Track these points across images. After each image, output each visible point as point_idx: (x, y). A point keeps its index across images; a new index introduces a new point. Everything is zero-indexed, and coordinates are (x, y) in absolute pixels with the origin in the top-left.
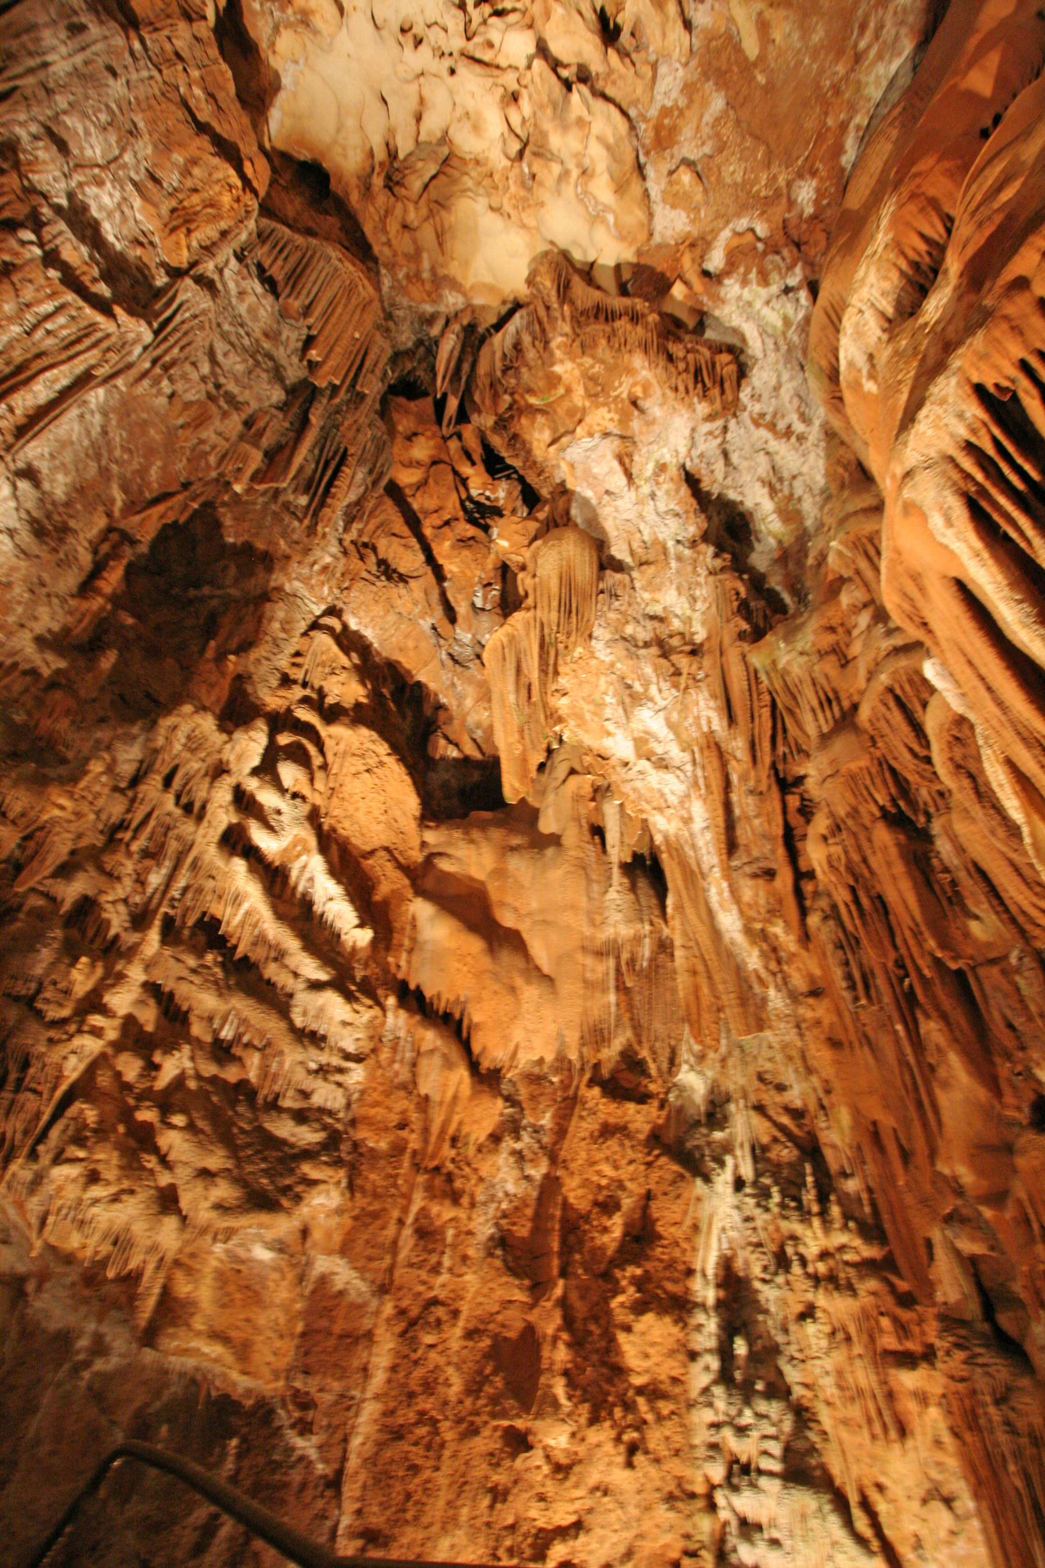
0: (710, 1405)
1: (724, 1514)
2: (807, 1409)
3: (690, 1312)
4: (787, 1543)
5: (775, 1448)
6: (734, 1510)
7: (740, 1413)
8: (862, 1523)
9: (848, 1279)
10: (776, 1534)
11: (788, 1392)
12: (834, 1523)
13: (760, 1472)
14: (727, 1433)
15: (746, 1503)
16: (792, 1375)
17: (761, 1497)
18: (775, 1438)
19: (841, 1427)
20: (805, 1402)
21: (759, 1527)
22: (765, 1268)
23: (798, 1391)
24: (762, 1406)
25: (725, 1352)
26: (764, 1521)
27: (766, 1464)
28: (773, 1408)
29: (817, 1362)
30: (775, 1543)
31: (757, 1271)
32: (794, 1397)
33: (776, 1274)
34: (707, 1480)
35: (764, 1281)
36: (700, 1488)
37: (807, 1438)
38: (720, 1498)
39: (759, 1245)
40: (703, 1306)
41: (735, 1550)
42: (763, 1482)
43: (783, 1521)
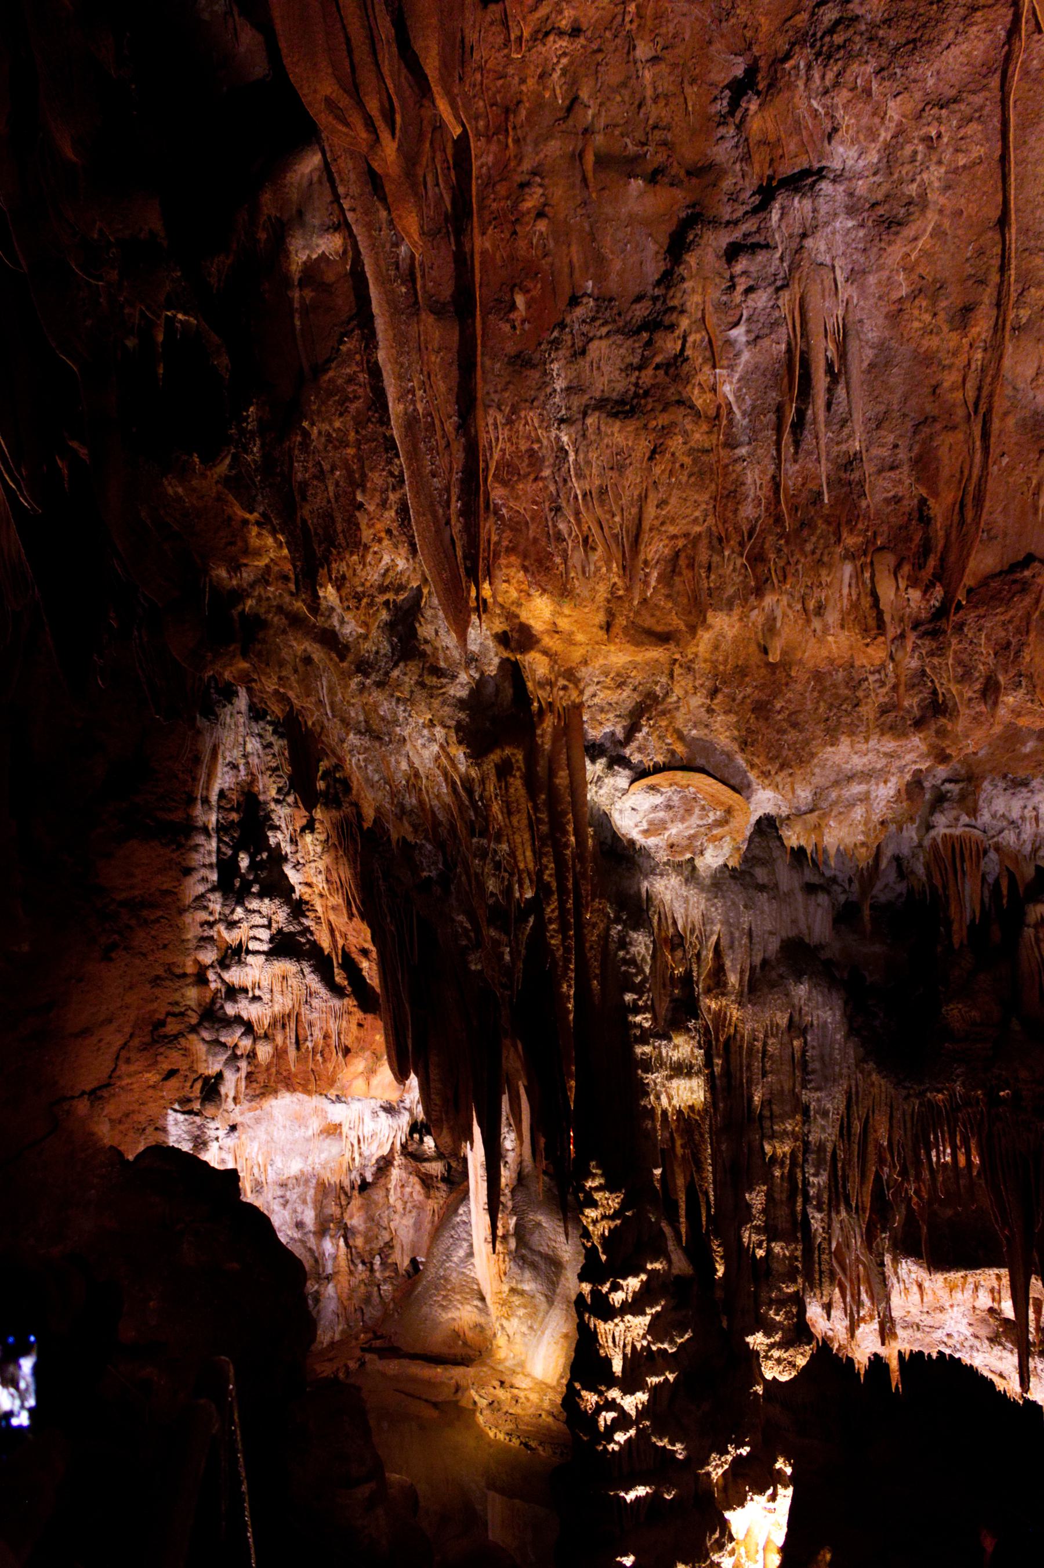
0: (206, 908)
1: (213, 986)
2: (307, 903)
3: (188, 837)
4: (266, 997)
5: (265, 934)
6: (223, 981)
7: (233, 912)
8: (340, 977)
9: (337, 794)
10: (257, 993)
11: (292, 889)
12: (313, 981)
13: (248, 952)
14: (221, 927)
15: (235, 976)
16: (294, 877)
17: (248, 969)
18: (269, 926)
19: (331, 912)
20: (306, 897)
21: (245, 990)
22: (279, 790)
23: (299, 891)
24: (254, 904)
25: (226, 867)
26: (249, 985)
27: (253, 946)
28: (266, 906)
29: (313, 865)
30: (256, 999)
31: (273, 793)
32: (296, 896)
33: (288, 794)
34: (197, 962)
35: (277, 801)
36: (190, 969)
37: (302, 924)
38: (211, 976)
39: (277, 769)
40: (205, 830)
41: (222, 1007)
42: (250, 959)
43: (265, 984)
